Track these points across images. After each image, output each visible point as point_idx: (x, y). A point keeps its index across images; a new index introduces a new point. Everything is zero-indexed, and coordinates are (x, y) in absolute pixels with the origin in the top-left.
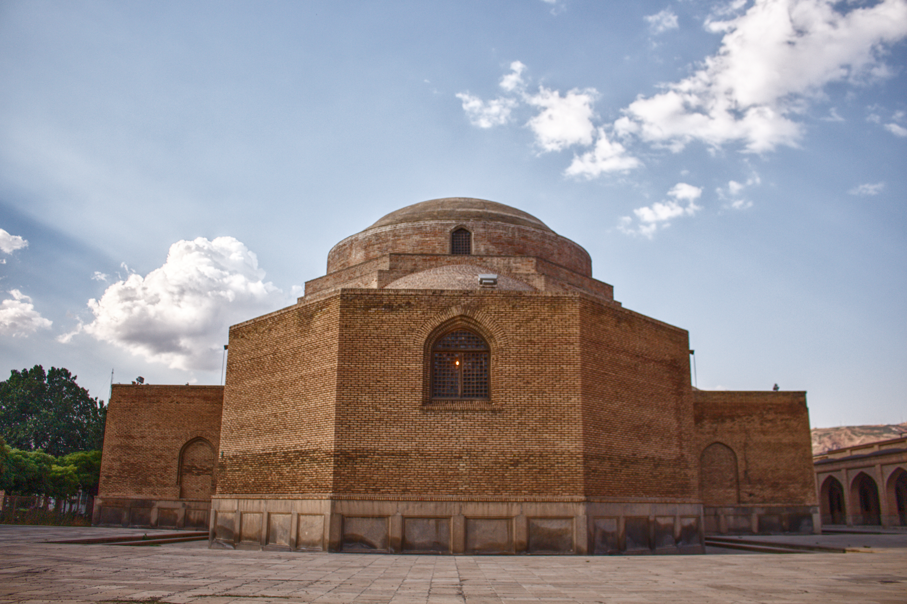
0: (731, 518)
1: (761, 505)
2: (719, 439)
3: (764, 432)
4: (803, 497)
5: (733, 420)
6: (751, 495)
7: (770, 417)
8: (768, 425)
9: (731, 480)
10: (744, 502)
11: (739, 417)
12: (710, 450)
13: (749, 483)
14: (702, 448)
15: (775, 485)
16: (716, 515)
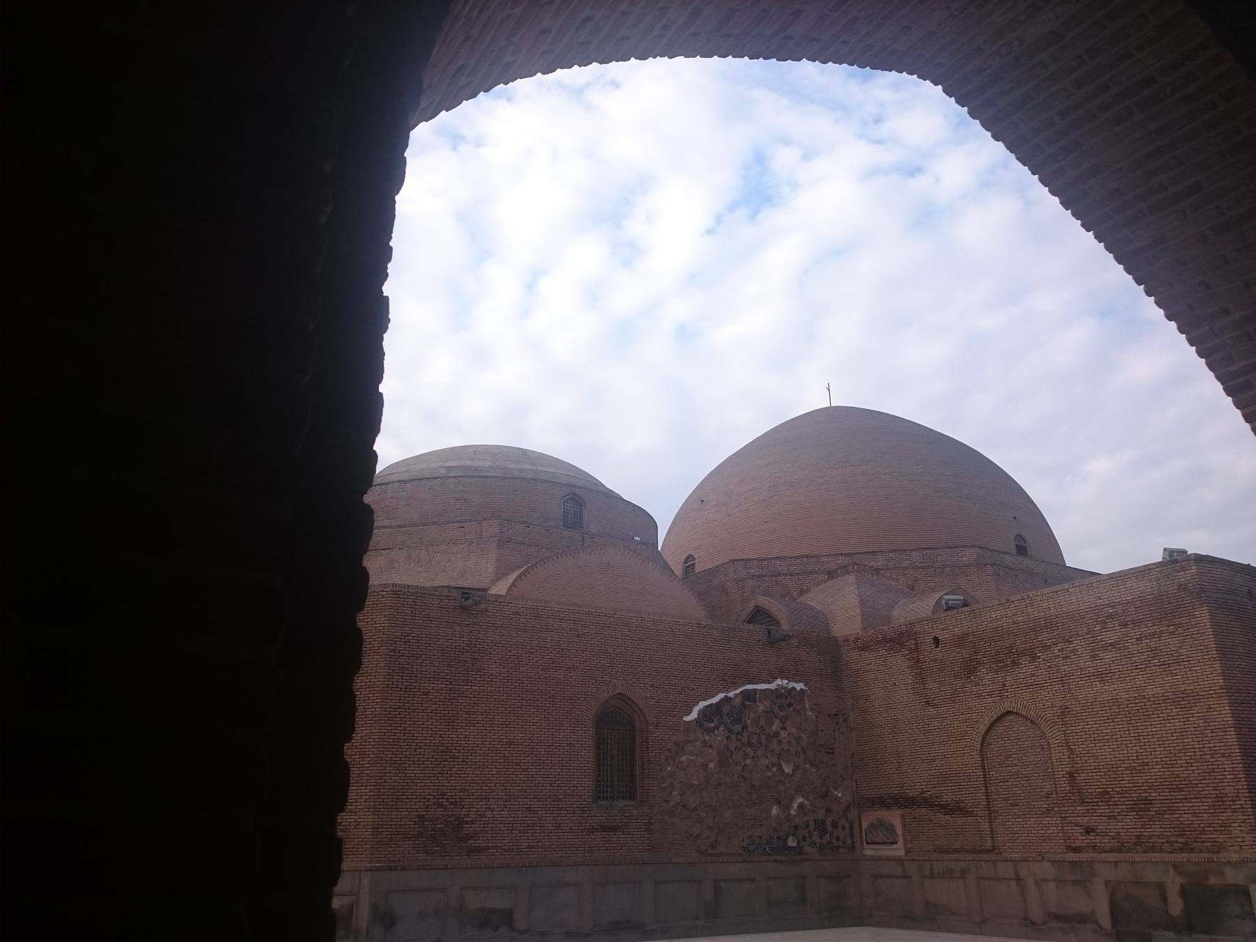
0: (1052, 885)
1: (1111, 857)
2: (1007, 706)
3: (1101, 676)
4: (1221, 838)
5: (1034, 658)
6: (1089, 830)
7: (1110, 637)
8: (1109, 656)
9: (1048, 795)
10: (1077, 850)
11: (1046, 648)
12: (1000, 729)
13: (1083, 803)
14: (983, 729)
15: (1141, 806)
16: (1018, 879)
